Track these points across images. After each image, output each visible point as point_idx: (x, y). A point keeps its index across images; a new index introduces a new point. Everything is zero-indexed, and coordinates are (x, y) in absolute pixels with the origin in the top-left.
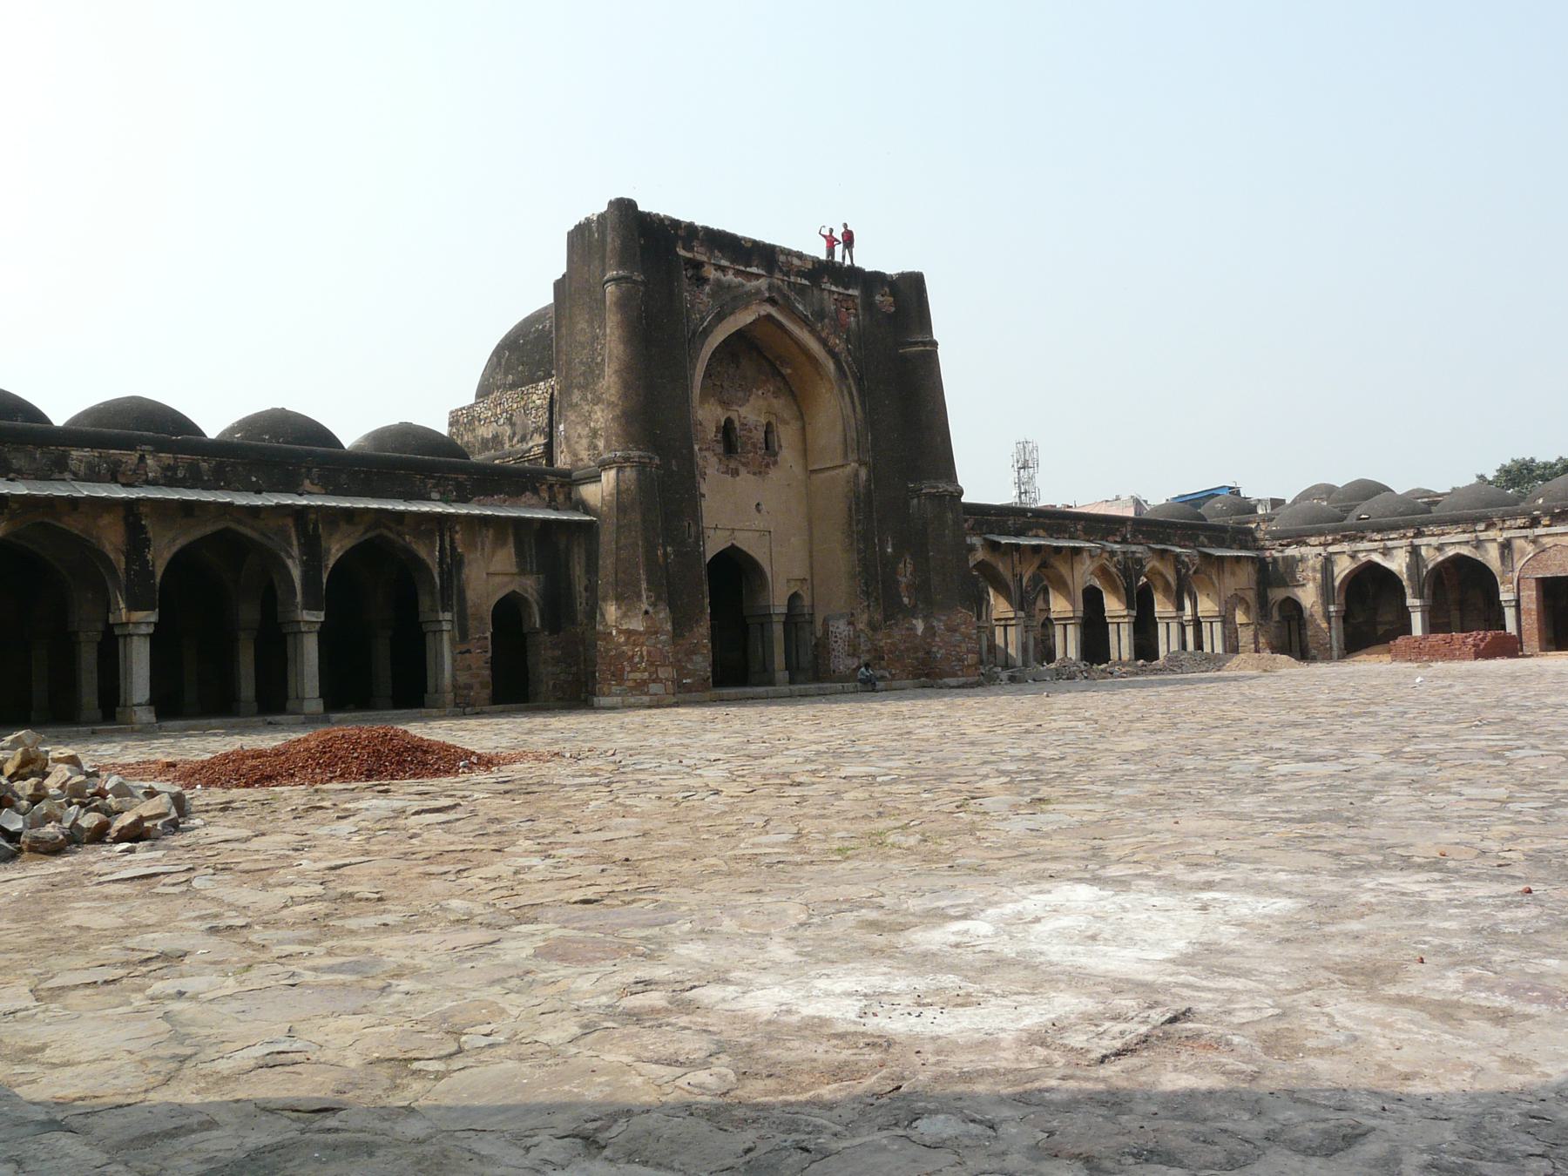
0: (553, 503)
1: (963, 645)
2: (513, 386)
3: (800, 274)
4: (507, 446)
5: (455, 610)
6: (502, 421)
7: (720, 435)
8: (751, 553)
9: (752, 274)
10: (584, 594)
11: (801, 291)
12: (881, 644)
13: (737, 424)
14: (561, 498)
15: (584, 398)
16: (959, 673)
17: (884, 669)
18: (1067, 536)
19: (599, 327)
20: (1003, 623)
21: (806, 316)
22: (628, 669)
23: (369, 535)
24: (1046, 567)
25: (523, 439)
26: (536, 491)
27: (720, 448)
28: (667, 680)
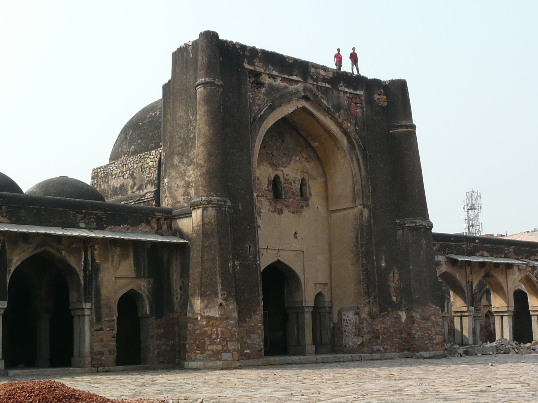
0: (160, 231)
1: (433, 329)
2: (134, 153)
3: (324, 80)
4: (129, 192)
5: (93, 301)
6: (127, 176)
7: (270, 187)
8: (291, 266)
9: (293, 80)
10: (179, 291)
11: (325, 91)
12: (378, 328)
13: (282, 180)
14: (165, 227)
15: (181, 161)
16: (431, 348)
17: (380, 345)
18: (503, 256)
19: (192, 115)
20: (459, 314)
21: (329, 108)
22: (208, 343)
23: (38, 251)
24: (489, 277)
25: (140, 188)
26: (148, 223)
27: (270, 195)
28: (234, 350)
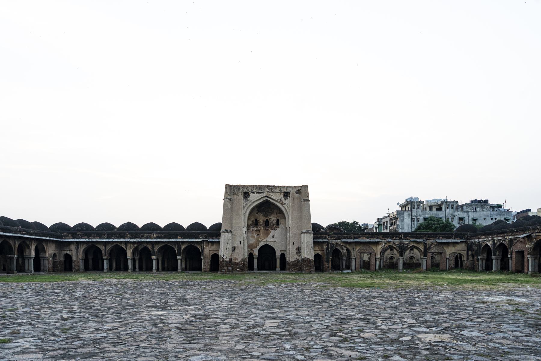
7: (264, 223)
27: (264, 225)
